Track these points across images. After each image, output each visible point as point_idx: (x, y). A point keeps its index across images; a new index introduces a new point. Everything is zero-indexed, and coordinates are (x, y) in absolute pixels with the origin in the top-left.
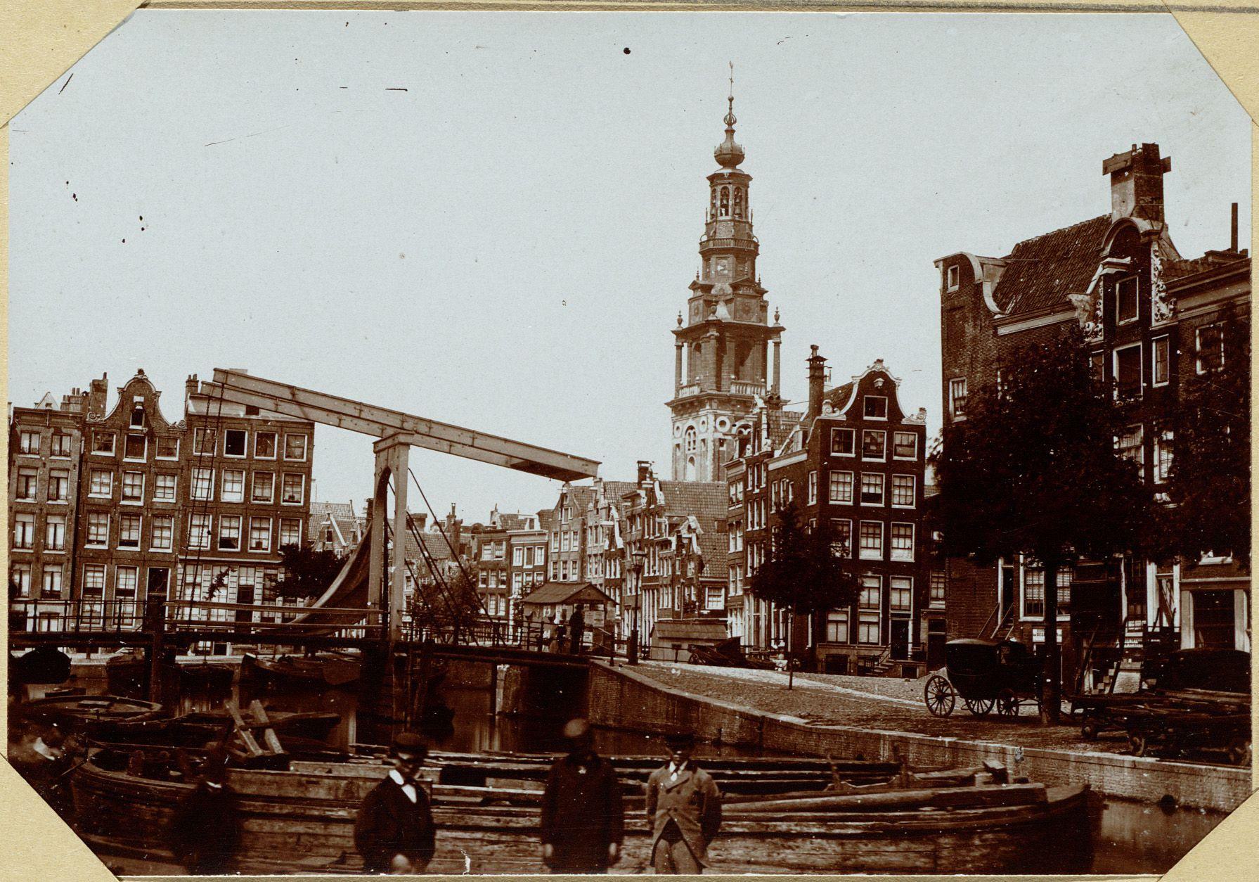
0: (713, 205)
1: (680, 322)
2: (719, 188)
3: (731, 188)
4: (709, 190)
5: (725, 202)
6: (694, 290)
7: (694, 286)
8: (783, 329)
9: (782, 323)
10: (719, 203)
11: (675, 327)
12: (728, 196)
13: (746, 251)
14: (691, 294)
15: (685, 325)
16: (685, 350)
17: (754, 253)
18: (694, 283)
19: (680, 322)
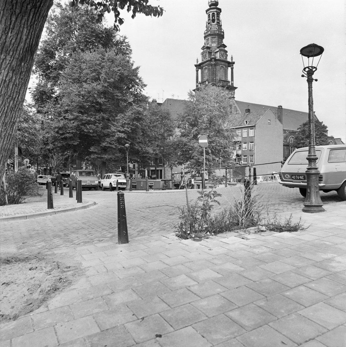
0: (209, 20)
1: (197, 62)
2: (211, 14)
3: (215, 13)
4: (207, 16)
5: (213, 18)
6: (203, 49)
7: (203, 48)
8: (234, 63)
9: (233, 61)
10: (211, 18)
11: (196, 63)
12: (215, 16)
13: (221, 36)
14: (202, 51)
15: (200, 61)
16: (200, 71)
17: (223, 38)
18: (204, 47)
19: (197, 62)
